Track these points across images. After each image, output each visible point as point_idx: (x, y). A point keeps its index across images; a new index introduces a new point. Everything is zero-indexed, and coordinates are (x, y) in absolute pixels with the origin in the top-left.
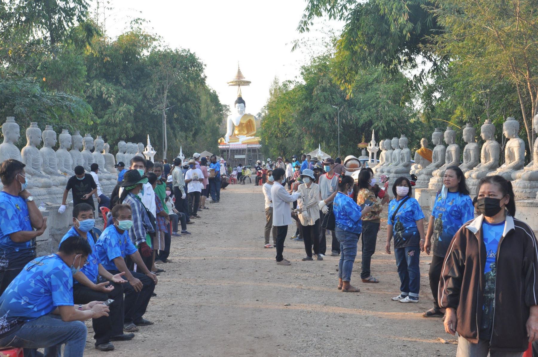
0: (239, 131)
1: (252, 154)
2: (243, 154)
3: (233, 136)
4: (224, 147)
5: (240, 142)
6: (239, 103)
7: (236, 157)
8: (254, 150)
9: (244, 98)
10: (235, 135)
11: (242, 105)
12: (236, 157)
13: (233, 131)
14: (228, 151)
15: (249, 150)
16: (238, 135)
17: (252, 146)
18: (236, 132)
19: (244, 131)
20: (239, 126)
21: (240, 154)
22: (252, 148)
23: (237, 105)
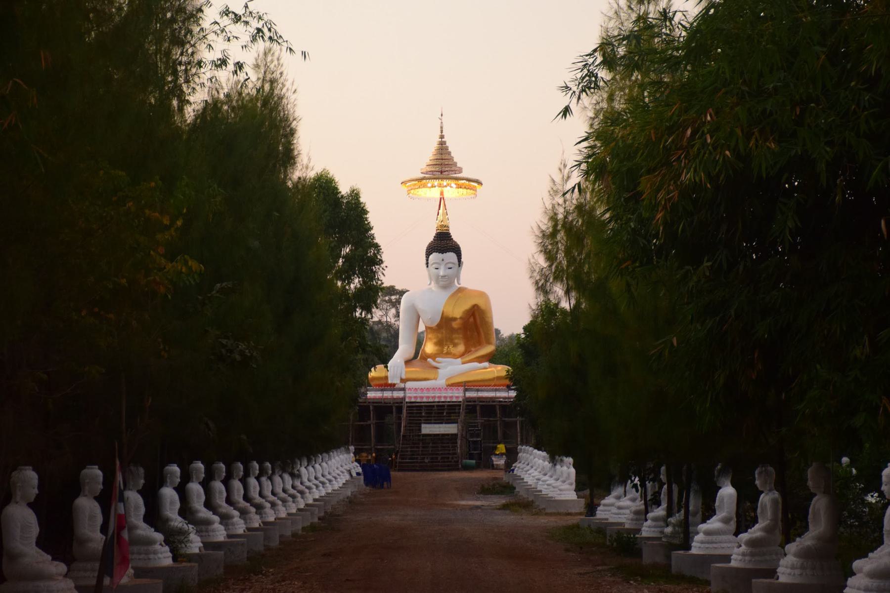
0: (440, 343)
1: (480, 420)
2: (449, 422)
3: (417, 356)
4: (388, 394)
5: (441, 382)
6: (442, 251)
7: (428, 429)
8: (487, 408)
9: (456, 236)
10: (425, 357)
11: (451, 256)
12: (428, 429)
13: (419, 344)
14: (399, 409)
15: (473, 407)
16: (433, 356)
17: (481, 394)
18: (429, 348)
19: (455, 345)
20: (440, 326)
21: (440, 421)
22: (480, 399)
23: (434, 257)
